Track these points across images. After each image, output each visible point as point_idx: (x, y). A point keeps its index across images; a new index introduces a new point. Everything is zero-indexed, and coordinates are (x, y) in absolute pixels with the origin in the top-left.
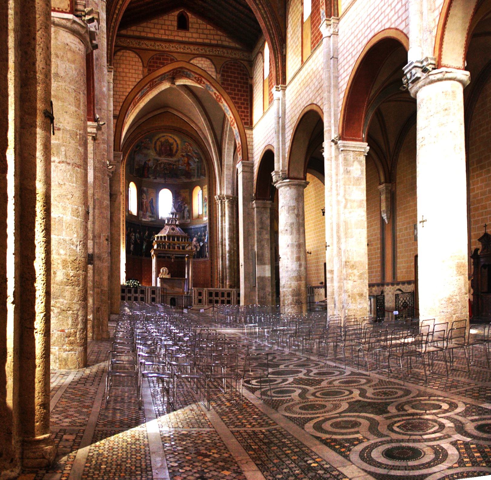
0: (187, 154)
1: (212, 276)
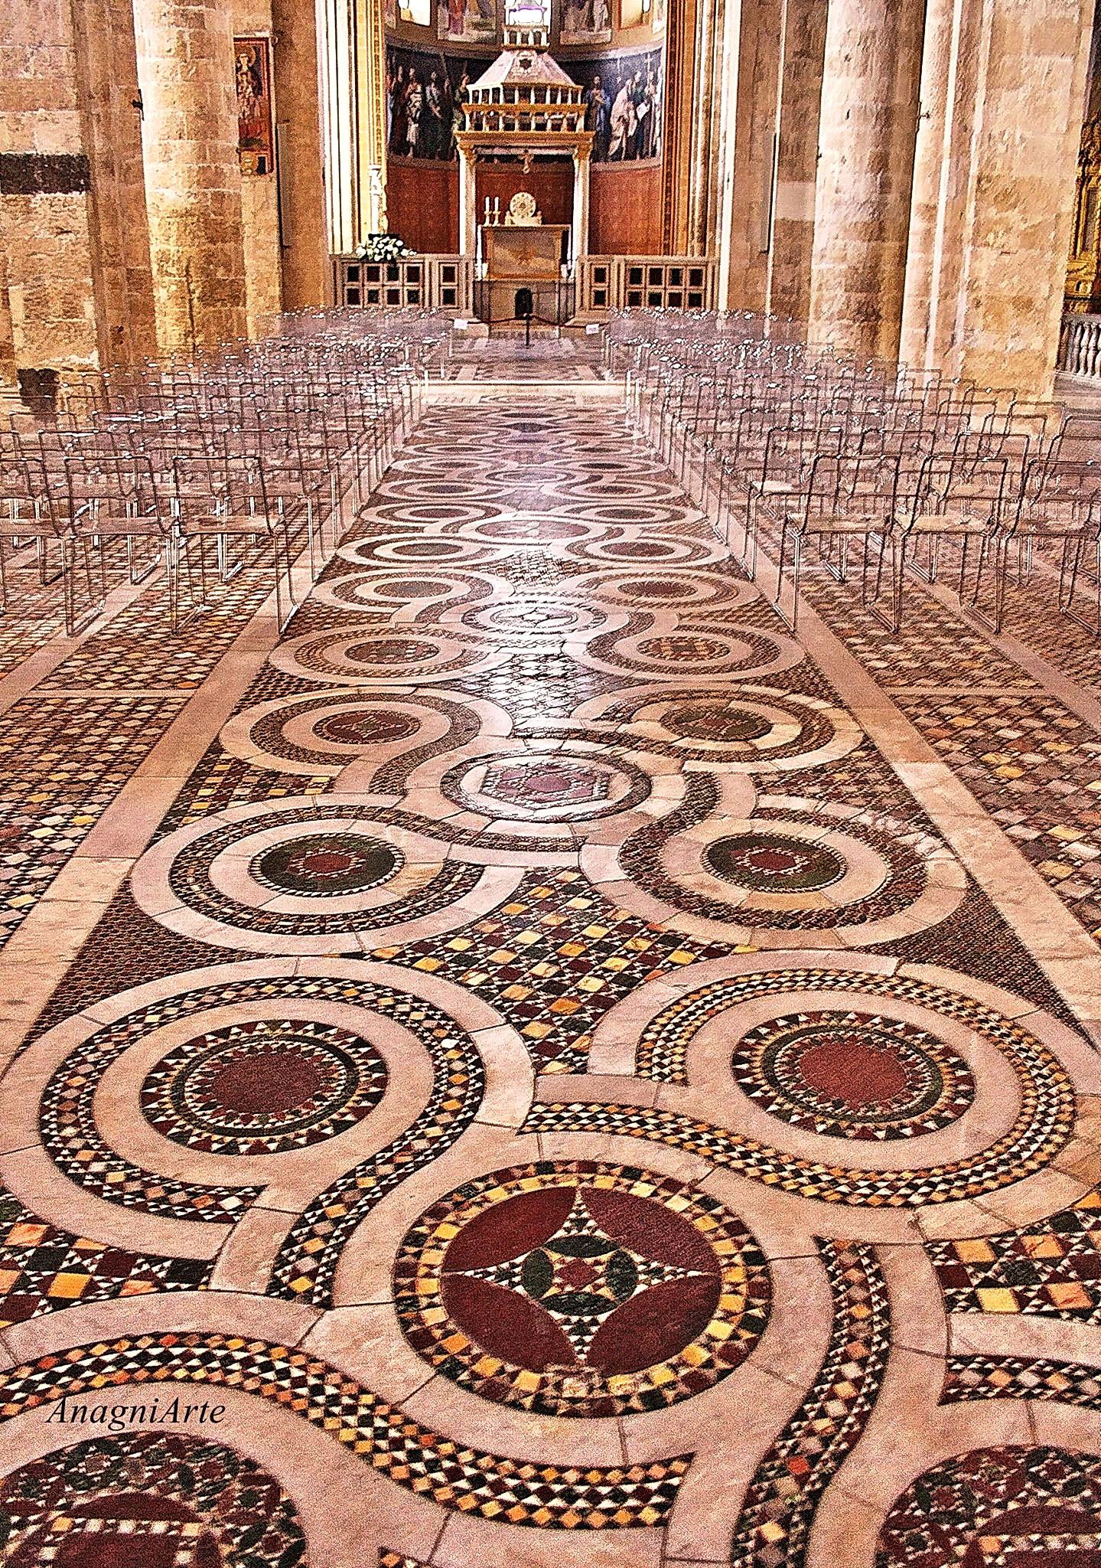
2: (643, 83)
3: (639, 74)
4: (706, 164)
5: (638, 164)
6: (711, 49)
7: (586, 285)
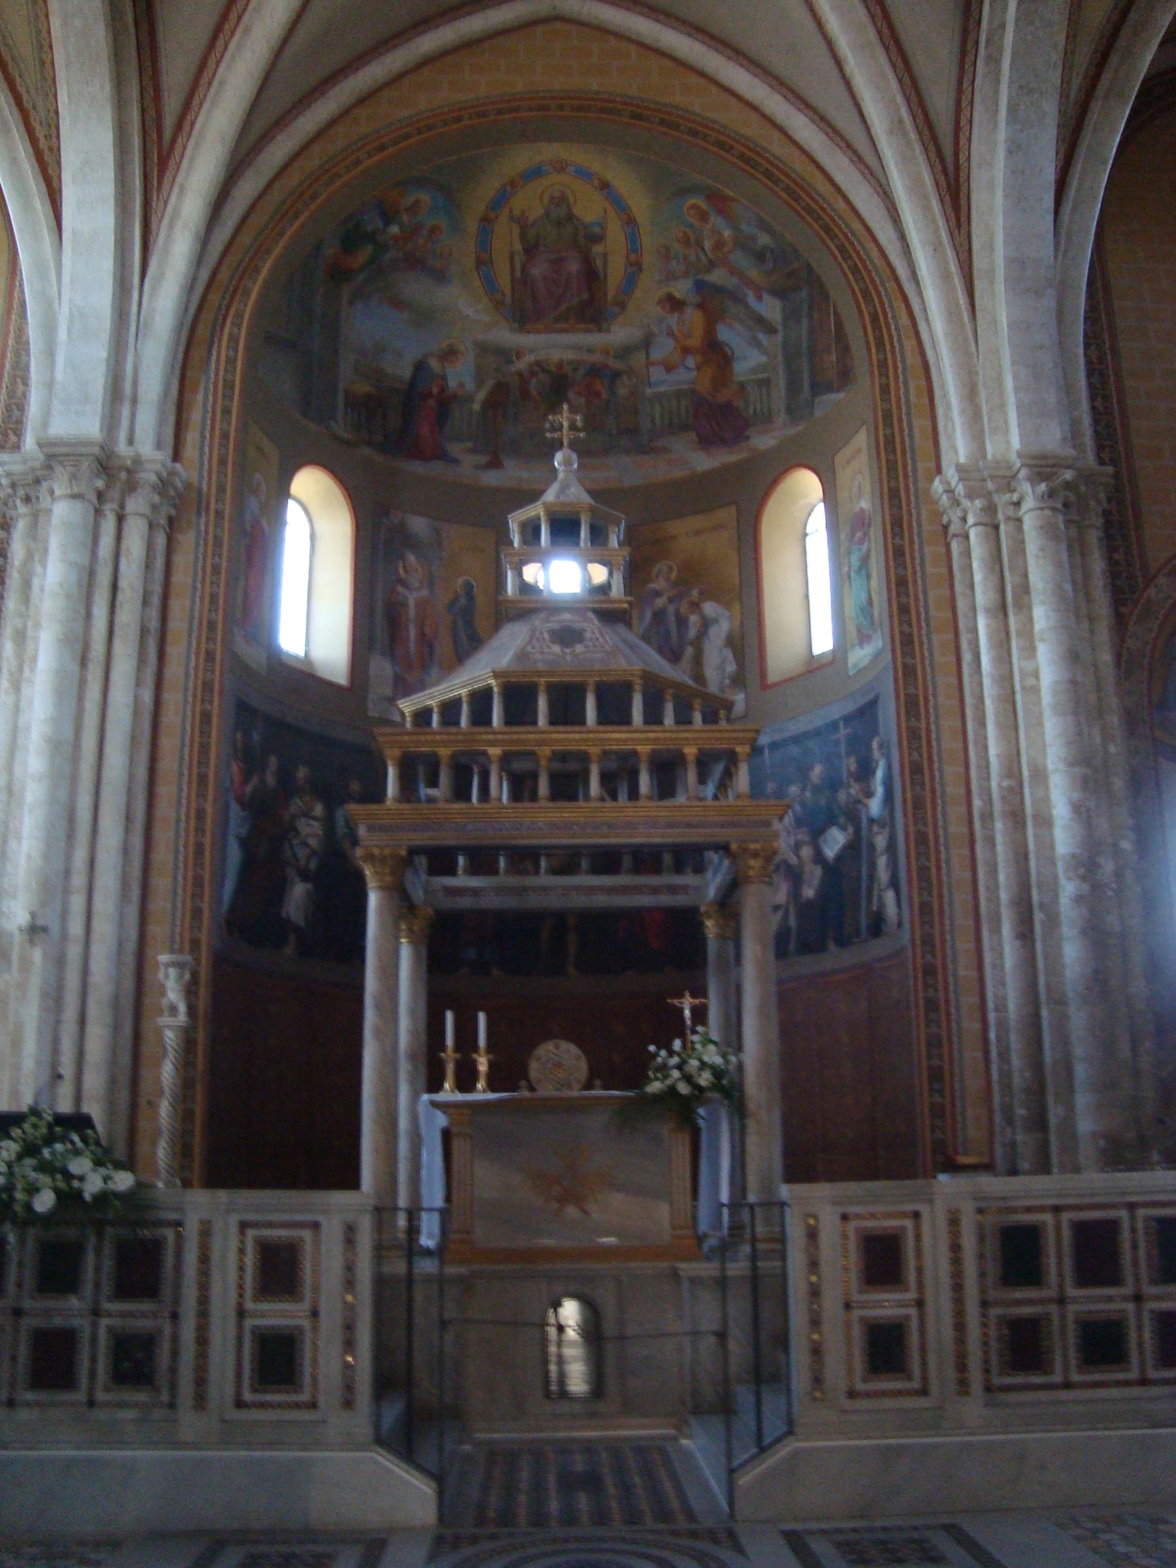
0: (700, 286)
1: (936, 1075)
2: (833, 784)
3: (817, 771)
4: (1025, 934)
5: (835, 959)
6: (1006, 679)
7: (831, 1304)
